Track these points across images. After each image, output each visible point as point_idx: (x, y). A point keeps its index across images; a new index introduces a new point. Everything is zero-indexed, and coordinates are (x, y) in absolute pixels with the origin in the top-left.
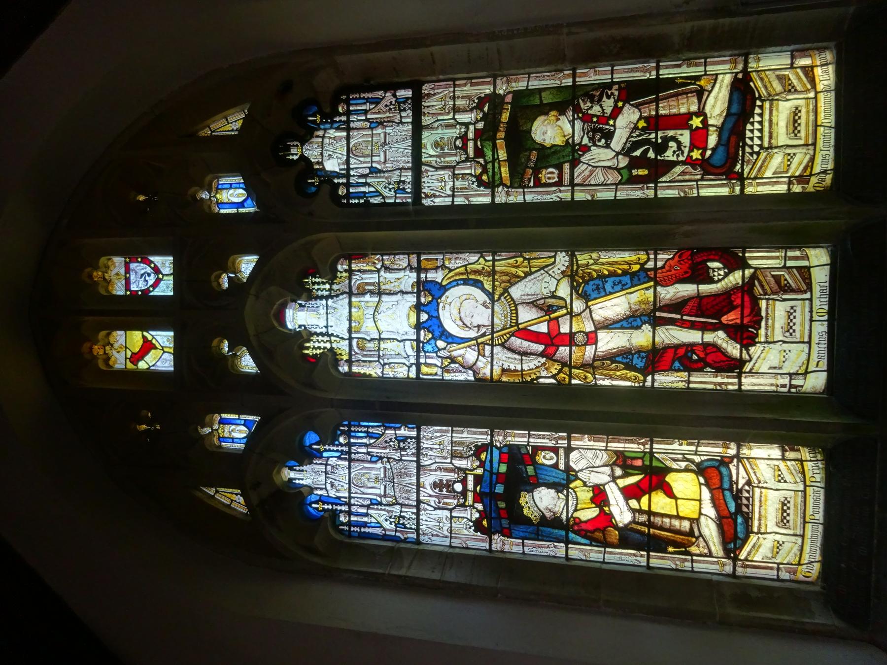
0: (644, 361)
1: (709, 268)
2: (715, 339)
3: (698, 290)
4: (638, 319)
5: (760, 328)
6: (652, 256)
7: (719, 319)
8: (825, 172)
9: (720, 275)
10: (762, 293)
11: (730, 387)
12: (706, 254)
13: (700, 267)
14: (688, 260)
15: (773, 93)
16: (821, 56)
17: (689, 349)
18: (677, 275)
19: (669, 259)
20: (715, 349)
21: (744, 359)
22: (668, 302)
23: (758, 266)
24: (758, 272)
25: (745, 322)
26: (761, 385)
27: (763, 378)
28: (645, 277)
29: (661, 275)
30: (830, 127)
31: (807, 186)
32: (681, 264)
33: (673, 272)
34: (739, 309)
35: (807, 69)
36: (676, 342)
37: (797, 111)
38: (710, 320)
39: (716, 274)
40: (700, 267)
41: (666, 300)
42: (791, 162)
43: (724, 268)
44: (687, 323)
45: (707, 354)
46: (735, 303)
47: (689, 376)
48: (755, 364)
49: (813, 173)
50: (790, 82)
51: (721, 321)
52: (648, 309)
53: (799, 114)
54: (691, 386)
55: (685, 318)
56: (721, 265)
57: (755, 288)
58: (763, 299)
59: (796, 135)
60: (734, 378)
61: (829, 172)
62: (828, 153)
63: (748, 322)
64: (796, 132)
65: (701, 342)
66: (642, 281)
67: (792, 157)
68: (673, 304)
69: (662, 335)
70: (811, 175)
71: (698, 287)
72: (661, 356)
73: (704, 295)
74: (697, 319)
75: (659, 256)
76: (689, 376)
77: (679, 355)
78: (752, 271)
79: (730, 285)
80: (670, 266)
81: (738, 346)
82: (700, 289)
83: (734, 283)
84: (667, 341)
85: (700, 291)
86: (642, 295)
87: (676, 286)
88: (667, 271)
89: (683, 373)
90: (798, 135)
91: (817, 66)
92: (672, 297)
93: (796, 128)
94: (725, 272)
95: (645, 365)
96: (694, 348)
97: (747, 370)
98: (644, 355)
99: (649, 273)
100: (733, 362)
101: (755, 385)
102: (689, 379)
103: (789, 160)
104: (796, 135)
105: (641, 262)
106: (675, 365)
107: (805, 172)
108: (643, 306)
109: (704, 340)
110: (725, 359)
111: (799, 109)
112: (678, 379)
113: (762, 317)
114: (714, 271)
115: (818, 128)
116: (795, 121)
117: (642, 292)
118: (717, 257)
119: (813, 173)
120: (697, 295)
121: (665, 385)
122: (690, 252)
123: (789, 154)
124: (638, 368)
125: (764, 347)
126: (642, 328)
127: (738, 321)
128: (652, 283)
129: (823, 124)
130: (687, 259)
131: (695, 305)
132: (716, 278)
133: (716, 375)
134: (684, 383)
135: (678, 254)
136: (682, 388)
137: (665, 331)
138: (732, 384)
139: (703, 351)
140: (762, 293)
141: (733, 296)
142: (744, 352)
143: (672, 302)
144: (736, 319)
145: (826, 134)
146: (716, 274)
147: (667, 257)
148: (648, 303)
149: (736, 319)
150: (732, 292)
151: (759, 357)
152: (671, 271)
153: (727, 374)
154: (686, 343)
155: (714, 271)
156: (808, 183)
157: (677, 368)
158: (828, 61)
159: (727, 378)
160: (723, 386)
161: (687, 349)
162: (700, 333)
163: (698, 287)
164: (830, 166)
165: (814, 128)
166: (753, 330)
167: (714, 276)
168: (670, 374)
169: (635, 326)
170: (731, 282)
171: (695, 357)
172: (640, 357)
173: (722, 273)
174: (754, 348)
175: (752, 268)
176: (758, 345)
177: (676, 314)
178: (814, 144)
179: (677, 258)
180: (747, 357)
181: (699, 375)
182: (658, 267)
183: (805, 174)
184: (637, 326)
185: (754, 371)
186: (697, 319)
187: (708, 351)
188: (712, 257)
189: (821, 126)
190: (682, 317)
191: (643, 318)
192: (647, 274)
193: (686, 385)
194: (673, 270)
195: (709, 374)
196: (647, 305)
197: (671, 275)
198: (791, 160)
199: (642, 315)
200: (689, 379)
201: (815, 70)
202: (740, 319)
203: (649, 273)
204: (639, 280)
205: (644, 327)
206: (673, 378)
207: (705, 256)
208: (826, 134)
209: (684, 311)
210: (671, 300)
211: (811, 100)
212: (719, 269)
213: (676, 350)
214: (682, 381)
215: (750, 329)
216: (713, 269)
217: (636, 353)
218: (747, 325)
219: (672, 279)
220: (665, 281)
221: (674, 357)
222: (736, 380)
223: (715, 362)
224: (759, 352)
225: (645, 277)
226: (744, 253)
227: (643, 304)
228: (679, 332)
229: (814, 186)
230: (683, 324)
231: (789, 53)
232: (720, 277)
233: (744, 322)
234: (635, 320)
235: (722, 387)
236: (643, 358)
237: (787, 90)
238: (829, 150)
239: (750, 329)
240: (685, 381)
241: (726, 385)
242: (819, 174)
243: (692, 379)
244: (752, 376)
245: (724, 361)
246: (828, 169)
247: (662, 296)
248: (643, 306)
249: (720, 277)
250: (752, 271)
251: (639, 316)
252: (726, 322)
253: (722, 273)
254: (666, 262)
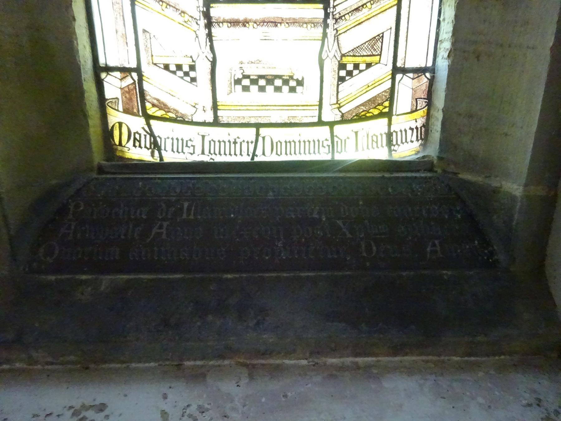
8: (155, 145)
15: (342, 25)
16: (409, 132)
30: (254, 155)
31: (121, 109)
35: (387, 104)
37: (293, 83)
42: (174, 73)
49: (152, 122)
50: (362, 67)
53: (286, 89)
59: (238, 82)
61: (156, 153)
62: (198, 150)
64: (246, 82)
67: (186, 74)
70: (148, 117)
90: (239, 88)
91: (390, 124)
93: (254, 82)
103: (179, 67)
104: (238, 82)
107: (154, 105)
111: (299, 89)
115: (254, 130)
116: (270, 80)
119: (152, 122)
123: (192, 68)
129: (260, 139)
145: (238, 146)
156: (127, 111)
158: (396, 148)
164: (169, 157)
165: (253, 121)
178: (216, 123)
183: (148, 105)
189: (258, 135)
198: (181, 74)
201: (384, 121)
208: (238, 146)
211: (316, 113)
229: (120, 124)
231: (430, 64)
237: (345, 60)
238: (203, 153)
242: (152, 134)
246: (163, 152)
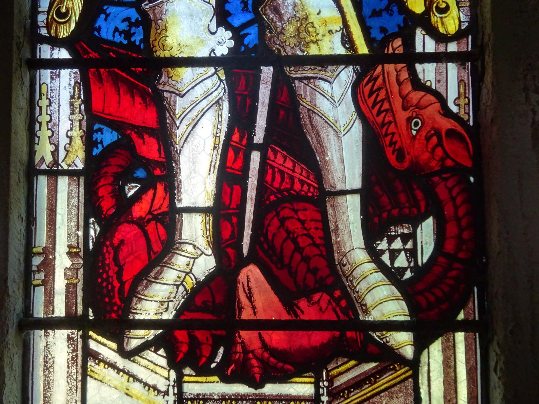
0: (119, 39)
1: (416, 222)
2: (190, 248)
3: (344, 193)
4: (249, 17)
5: (226, 379)
6: (452, 47)
7: (252, 258)
9: (393, 258)
10: (337, 383)
11: (39, 294)
12: (461, 212)
13: (419, 195)
14: (442, 160)
17: (158, 172)
18: (392, 129)
19: (442, 100)
20: (157, 247)
21: (127, 334)
22: (306, 103)
23: (424, 369)
24: (402, 372)
25: (244, 334)
26: (48, 386)
27: (70, 392)
28: (383, 30)
29: (393, 79)
32: (428, 139)
33: (402, 116)
34: (285, 317)
36: (179, 132)
38: (248, 232)
39: (397, 244)
40: (419, 195)
41: (313, 100)
43: (415, 269)
44: (239, 164)
45: (141, 223)
46: (303, 303)
47: (71, 174)
48: (112, 366)
51: (244, 262)
52: (283, 44)
54: (42, 182)
55: (256, 157)
56: (425, 261)
57: (353, 363)
58: (317, 388)
60: (68, 306)
63: (243, 343)
65: (179, 205)
66: (371, 22)
68: (298, 119)
69: (199, 91)
71: (352, 192)
72: (132, 89)
73: (330, 211)
74: (251, 194)
75: (452, 69)
76: (71, 174)
77: (137, 141)
78: (409, 352)
79: (362, 287)
80: (419, 106)
81: (168, 316)
82: (349, 197)
83: (369, 300)
84: (180, 105)
85: (340, 199)
86: (325, 23)
87: (357, 129)
88: (404, 98)
89: (81, 154)
92: (322, 116)
94: (402, 270)
95: (107, 42)
96: (160, 188)
97: (93, 345)
98: (138, 36)
99: (398, 42)
100: (117, 300)
101: (48, 368)
102: (64, 173)
105: (435, 18)
106: (106, 129)
108: (291, 29)
109: (185, 216)
110: (127, 276)
112: (63, 141)
113: (262, 387)
114: (405, 238)
117: (338, 25)
118: (450, 246)
120: (328, 188)
121: (44, 103)
122: (468, 164)
124: (95, 21)
125: (166, 393)
126: (221, 30)
127: (247, 315)
128: (363, 49)
130: (447, 155)
131: (297, 186)
132: (383, 245)
133: (77, 254)
134: (49, 158)
135: (459, 129)
136: (32, 153)
137: (215, 96)
138: (49, 301)
139: (150, 212)
140: (337, 383)
141: (326, 297)
142: (151, 334)
143: (304, 114)
144: (254, 308)
146: (397, 244)
147: (452, 95)
148: (302, 43)
149: (254, 308)
150: (337, 293)
151: (136, 379)
152: (405, 108)
153: (80, 286)
154: (177, 162)
155: (405, 238)
157: (97, 136)
159: (68, 286)
160: (42, 275)
161: (158, 164)
162: (208, 202)
163: (352, 192)
166: (218, 359)
167: (391, 240)
168: (77, 117)
169: (228, 7)
170: (370, 290)
171: (131, 190)
172: (131, 25)
173: (401, 261)
174: (163, 362)
175: (418, 353)
176: (173, 375)
177: (267, 130)
179: (446, 124)
180: (134, 343)
181: (74, 202)
182: (419, 67)
184: (229, 14)
185: (91, 363)
186: (251, 194)
187: (150, 227)
188: (452, 229)
190: (257, 147)
191: (253, 32)
192: (394, 36)
193: (44, 167)
194: (408, 114)
195: (80, 233)
196: (293, 41)
197: (391, 110)
199: (263, 28)
200: (64, 173)
202: (252, 317)
203: (398, 42)
204: (376, 14)
205: (225, 35)
206: (64, 126)
207: (456, 208)
209: (275, 153)
210: (312, 111)
212: (412, 254)
213: (151, 132)
214: (55, 153)
215: (221, 350)
216: (413, 236)
217: (143, 14)
218: (235, 344)
219: (379, 113)
220: (370, 95)
221: (133, 127)
222: (60, 311)
223: (117, 250)
224: (152, 379)
225: (383, 30)
226: (463, 326)
227: (298, 30)
228: (210, 143)
230: (237, 151)
232: (386, 258)
233: (243, 333)
234: (245, 8)
235: (39, 271)
236: (128, 35)
239: (221, 350)
240: (56, 162)
241: (44, 283)
243: (63, 182)
244: (74, 359)
245: (119, 274)
247: (324, 85)
248: (291, 29)
249: (386, 258)
250: (409, 352)
251: (258, 20)
252: (242, 277)
253: (401, 261)
254: (436, 94)
